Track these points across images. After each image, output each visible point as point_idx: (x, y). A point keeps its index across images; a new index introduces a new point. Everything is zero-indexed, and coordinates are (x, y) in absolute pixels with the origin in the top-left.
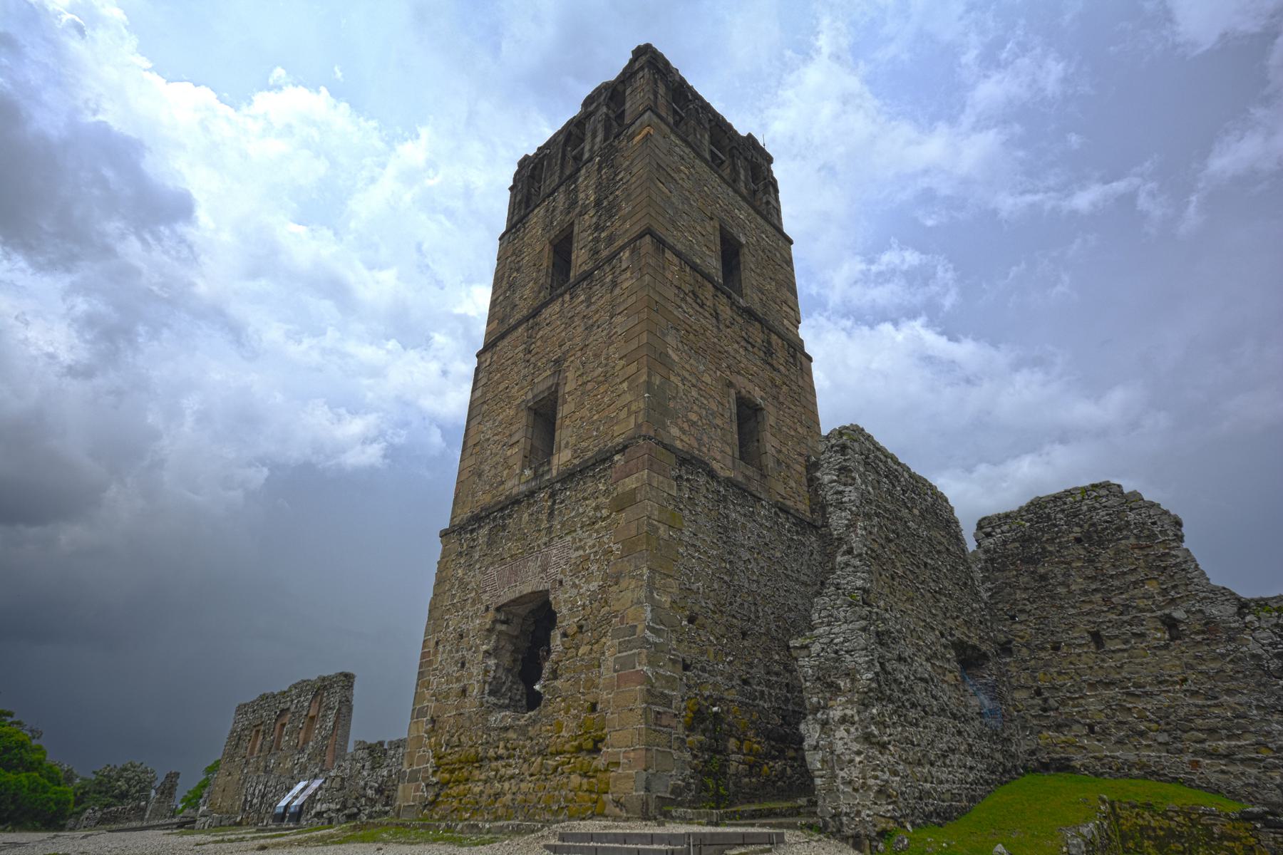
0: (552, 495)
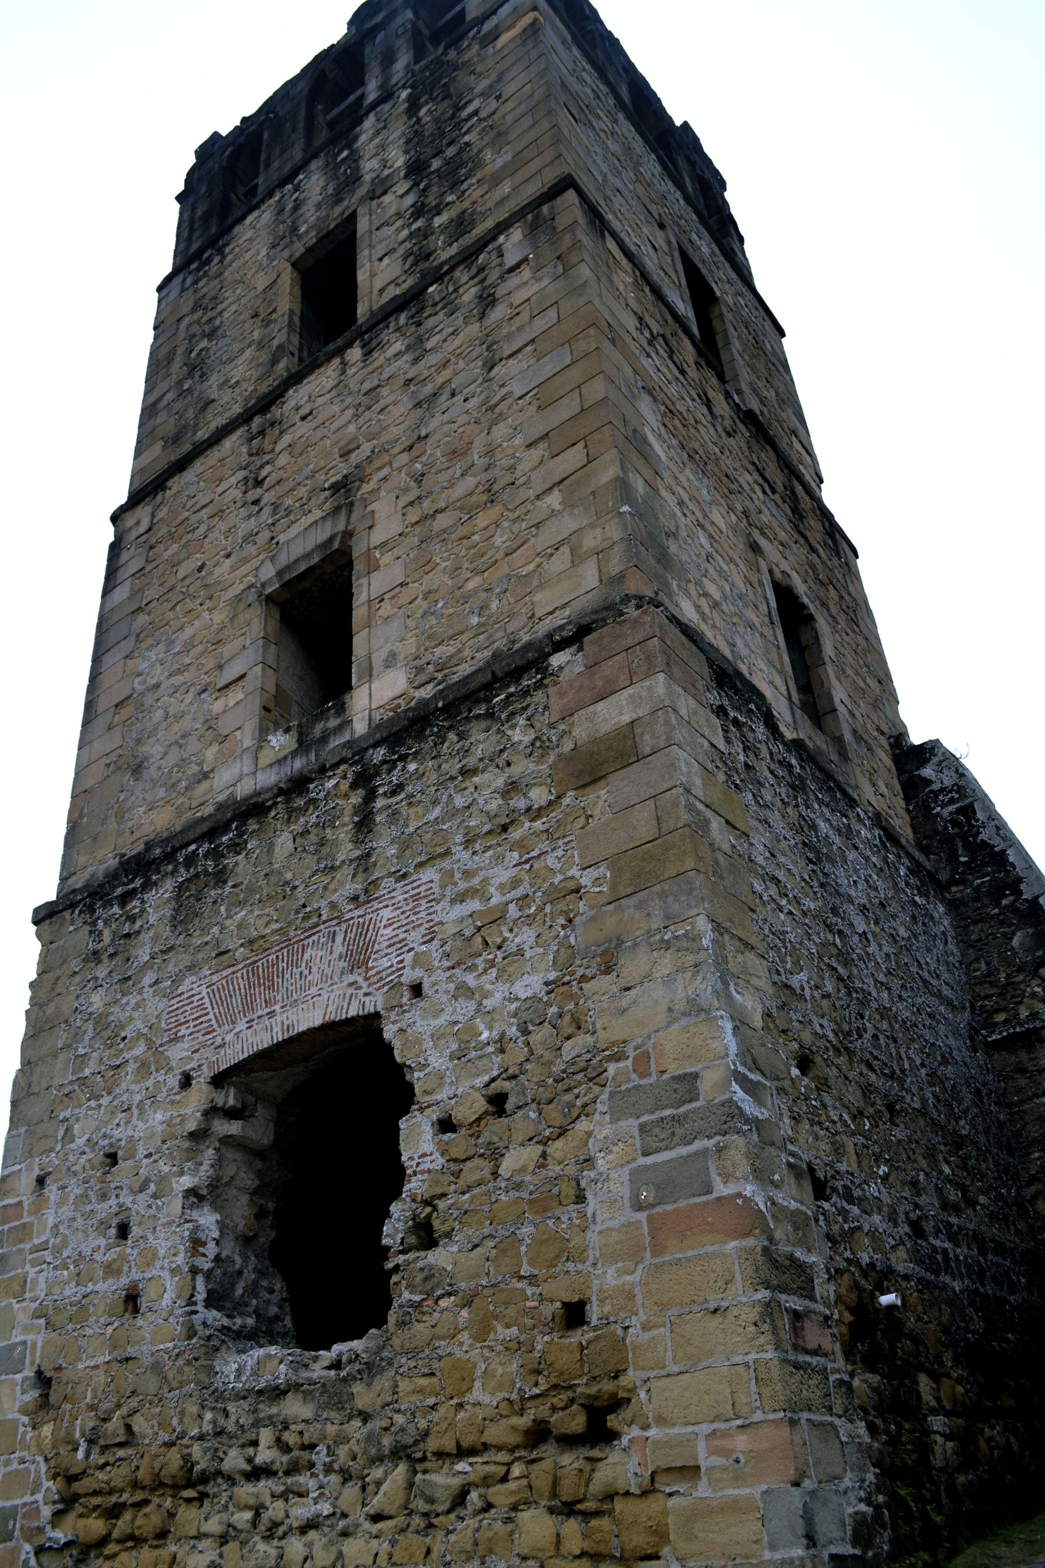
0: (365, 780)
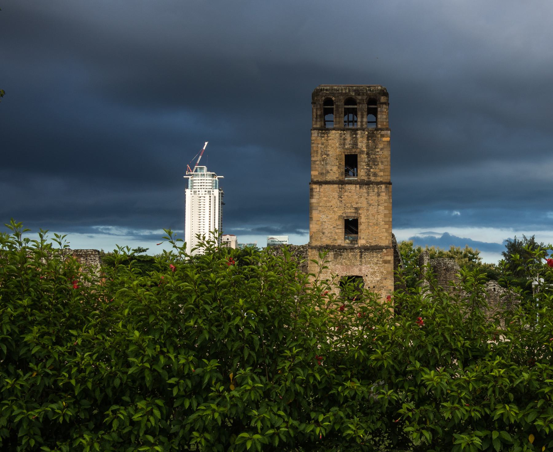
0: (361, 252)
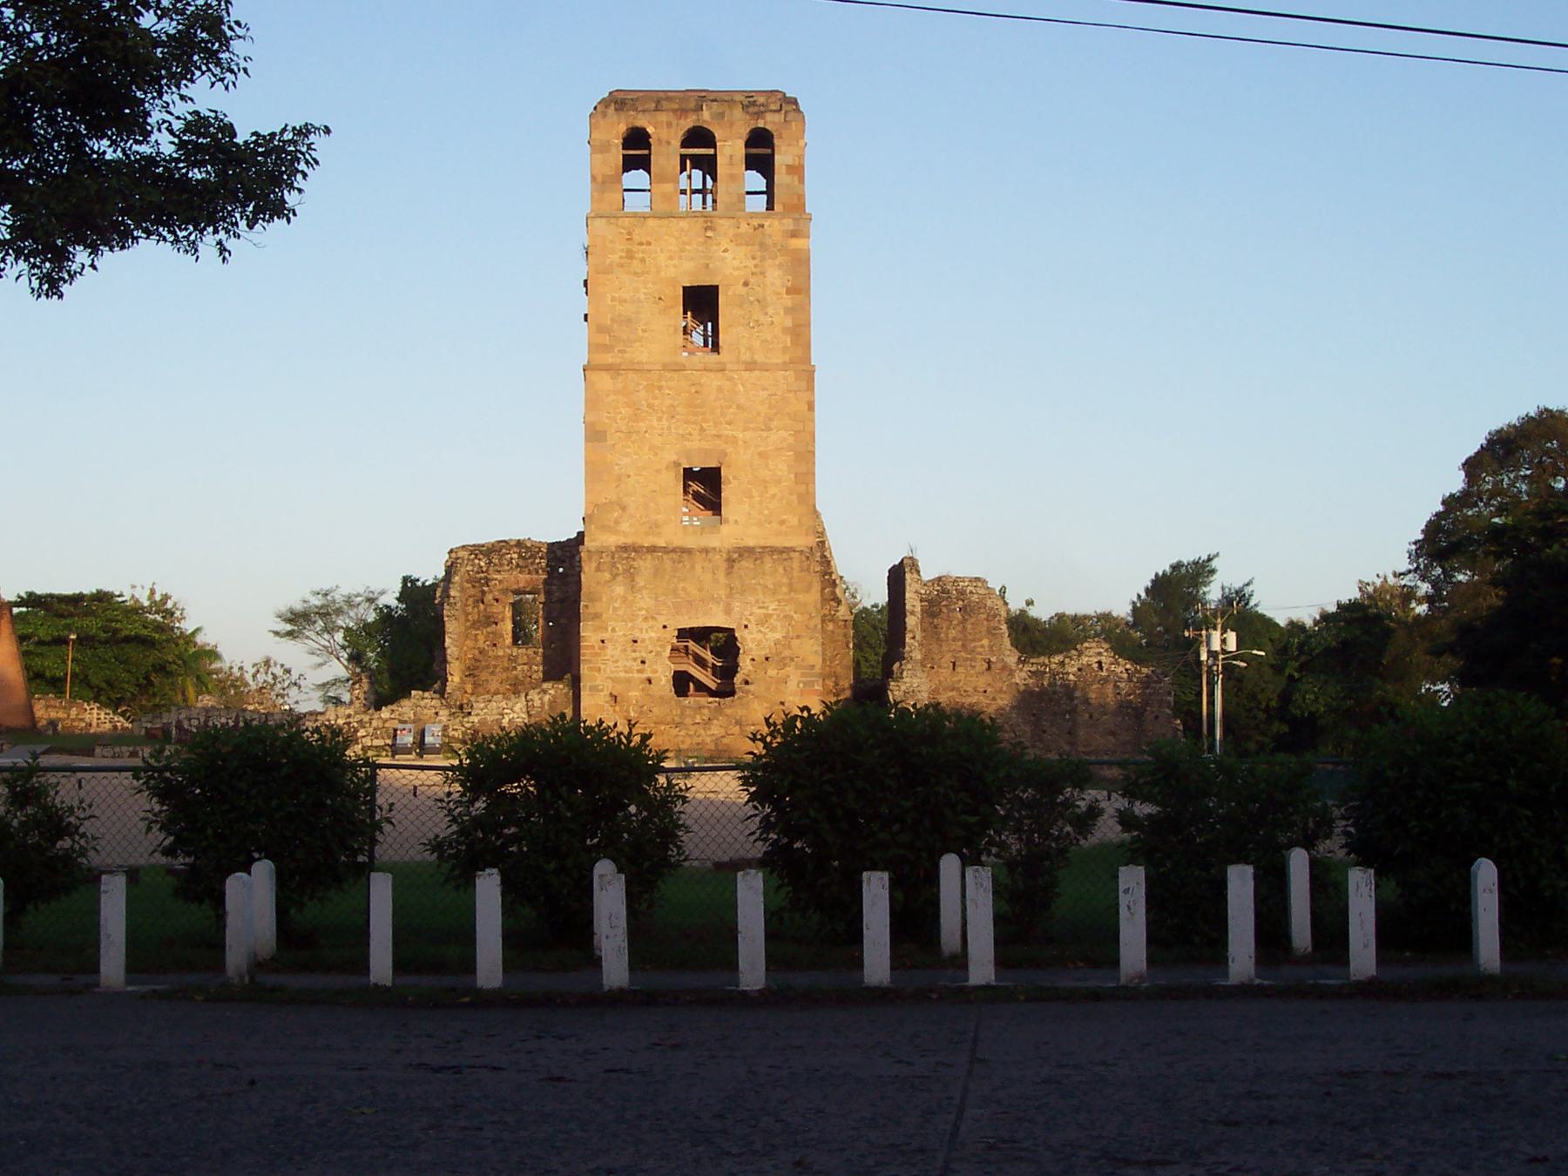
0: (731, 562)
